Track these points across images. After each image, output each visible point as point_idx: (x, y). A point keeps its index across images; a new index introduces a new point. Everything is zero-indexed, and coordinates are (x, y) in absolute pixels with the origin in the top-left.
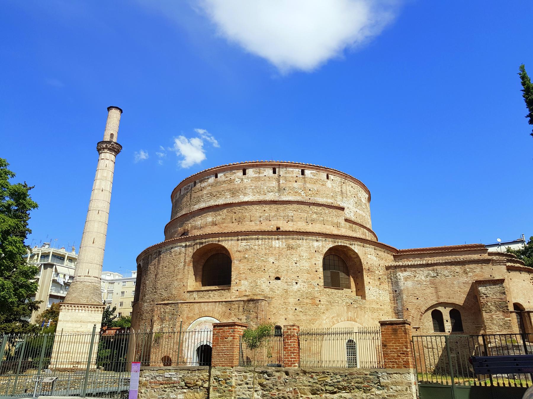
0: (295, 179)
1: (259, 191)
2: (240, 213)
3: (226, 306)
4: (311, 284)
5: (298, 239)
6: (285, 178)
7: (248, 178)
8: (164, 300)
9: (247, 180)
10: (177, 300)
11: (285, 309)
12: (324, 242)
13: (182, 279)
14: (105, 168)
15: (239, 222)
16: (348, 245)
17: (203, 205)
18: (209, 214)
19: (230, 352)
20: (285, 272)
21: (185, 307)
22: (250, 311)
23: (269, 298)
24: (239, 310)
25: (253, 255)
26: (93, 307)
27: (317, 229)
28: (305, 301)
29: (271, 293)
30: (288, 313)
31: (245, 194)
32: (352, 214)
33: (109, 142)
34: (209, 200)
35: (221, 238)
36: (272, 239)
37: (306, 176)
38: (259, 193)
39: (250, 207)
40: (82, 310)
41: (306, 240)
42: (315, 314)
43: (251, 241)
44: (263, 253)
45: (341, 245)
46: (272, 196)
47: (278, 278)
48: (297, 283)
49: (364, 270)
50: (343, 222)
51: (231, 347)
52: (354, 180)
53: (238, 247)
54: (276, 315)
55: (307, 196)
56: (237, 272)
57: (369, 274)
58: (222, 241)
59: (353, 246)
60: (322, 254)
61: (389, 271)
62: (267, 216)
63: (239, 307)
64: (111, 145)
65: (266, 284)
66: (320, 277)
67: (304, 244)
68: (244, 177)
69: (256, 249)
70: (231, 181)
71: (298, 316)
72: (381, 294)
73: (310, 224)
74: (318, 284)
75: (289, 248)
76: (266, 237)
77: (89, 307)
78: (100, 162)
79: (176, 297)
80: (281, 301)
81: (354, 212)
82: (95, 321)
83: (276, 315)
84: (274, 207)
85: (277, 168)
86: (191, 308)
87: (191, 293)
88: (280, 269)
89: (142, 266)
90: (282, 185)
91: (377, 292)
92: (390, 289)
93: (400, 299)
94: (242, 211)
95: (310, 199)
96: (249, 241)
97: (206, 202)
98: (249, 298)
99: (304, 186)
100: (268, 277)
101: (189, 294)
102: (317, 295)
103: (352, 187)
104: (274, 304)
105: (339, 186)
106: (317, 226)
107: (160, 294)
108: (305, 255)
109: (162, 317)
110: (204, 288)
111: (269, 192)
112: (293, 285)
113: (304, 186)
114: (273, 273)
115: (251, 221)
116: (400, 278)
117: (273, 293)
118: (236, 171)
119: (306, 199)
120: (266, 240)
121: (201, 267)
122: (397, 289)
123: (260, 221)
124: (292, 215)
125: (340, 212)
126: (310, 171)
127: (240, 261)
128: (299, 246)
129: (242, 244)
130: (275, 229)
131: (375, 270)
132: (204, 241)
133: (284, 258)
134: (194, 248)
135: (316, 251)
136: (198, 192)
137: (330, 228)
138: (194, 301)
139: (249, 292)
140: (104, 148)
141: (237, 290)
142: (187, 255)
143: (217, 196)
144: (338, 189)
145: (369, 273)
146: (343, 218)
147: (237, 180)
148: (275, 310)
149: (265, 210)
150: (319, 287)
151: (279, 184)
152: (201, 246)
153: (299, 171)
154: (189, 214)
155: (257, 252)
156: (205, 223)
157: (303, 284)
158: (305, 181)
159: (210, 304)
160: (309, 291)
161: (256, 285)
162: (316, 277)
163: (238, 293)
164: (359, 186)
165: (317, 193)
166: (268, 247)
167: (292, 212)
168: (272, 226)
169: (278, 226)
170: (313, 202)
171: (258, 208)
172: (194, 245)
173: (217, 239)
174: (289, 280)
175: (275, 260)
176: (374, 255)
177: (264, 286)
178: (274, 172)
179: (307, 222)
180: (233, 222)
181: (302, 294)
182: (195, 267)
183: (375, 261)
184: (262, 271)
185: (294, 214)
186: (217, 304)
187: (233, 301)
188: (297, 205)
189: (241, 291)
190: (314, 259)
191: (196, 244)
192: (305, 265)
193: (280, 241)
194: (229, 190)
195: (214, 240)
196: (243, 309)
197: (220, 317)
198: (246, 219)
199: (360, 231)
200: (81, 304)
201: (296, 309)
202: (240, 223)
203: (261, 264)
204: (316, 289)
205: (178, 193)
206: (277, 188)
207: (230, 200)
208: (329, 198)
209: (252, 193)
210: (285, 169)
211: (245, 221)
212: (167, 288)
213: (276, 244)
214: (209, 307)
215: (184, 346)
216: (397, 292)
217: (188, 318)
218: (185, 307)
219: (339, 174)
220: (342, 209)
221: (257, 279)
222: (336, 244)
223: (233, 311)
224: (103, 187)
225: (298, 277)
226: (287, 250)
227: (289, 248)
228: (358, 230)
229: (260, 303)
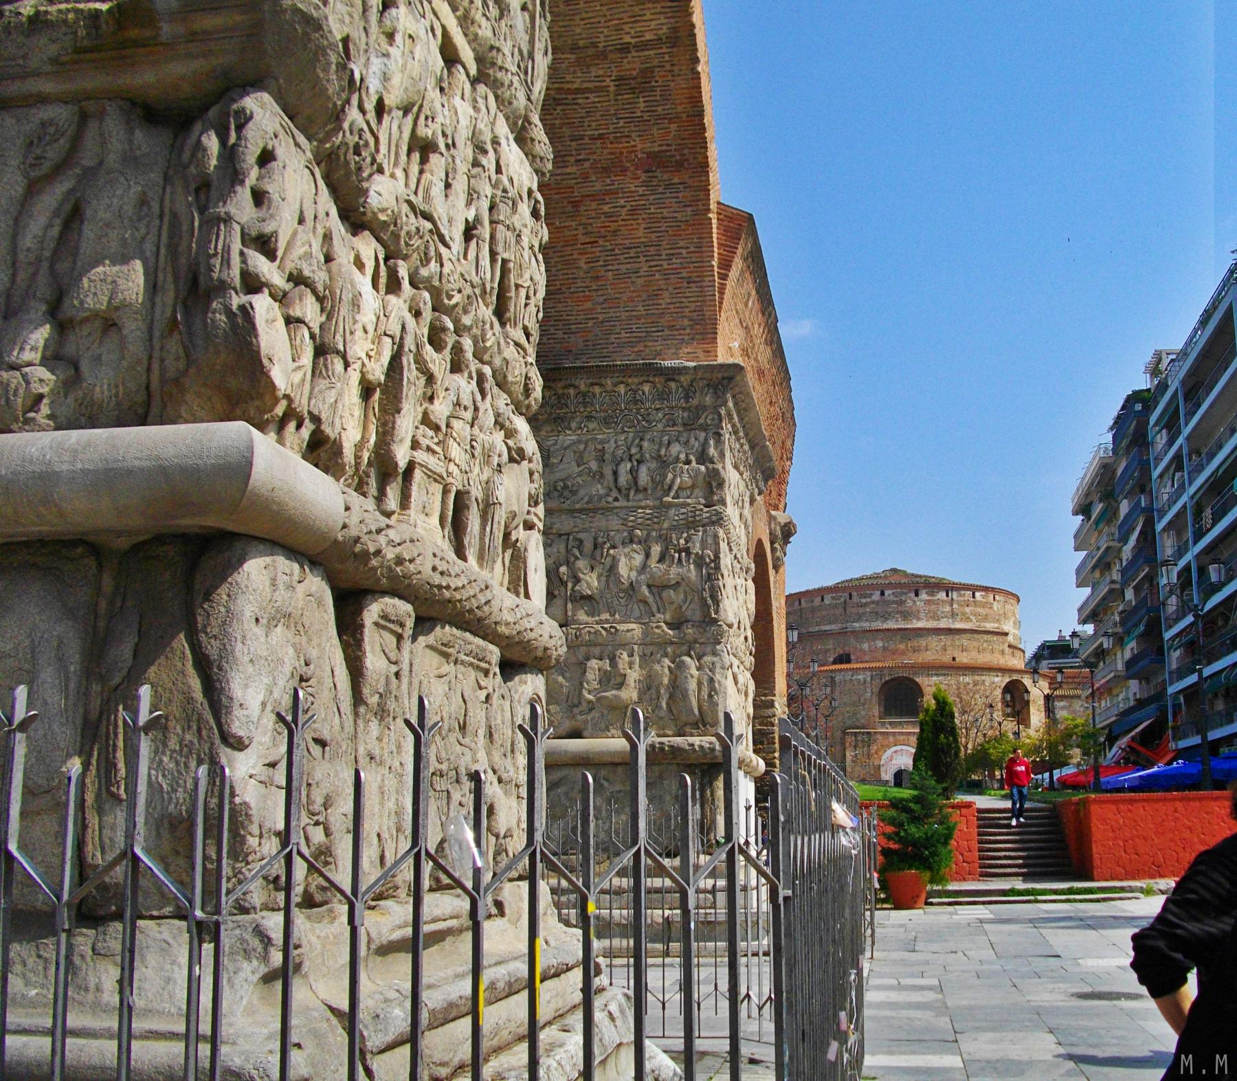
7: (921, 601)
17: (866, 625)
31: (919, 619)
38: (933, 618)
50: (1007, 650)
68: (916, 599)
178: (947, 595)
205: (819, 599)
220: (1006, 634)
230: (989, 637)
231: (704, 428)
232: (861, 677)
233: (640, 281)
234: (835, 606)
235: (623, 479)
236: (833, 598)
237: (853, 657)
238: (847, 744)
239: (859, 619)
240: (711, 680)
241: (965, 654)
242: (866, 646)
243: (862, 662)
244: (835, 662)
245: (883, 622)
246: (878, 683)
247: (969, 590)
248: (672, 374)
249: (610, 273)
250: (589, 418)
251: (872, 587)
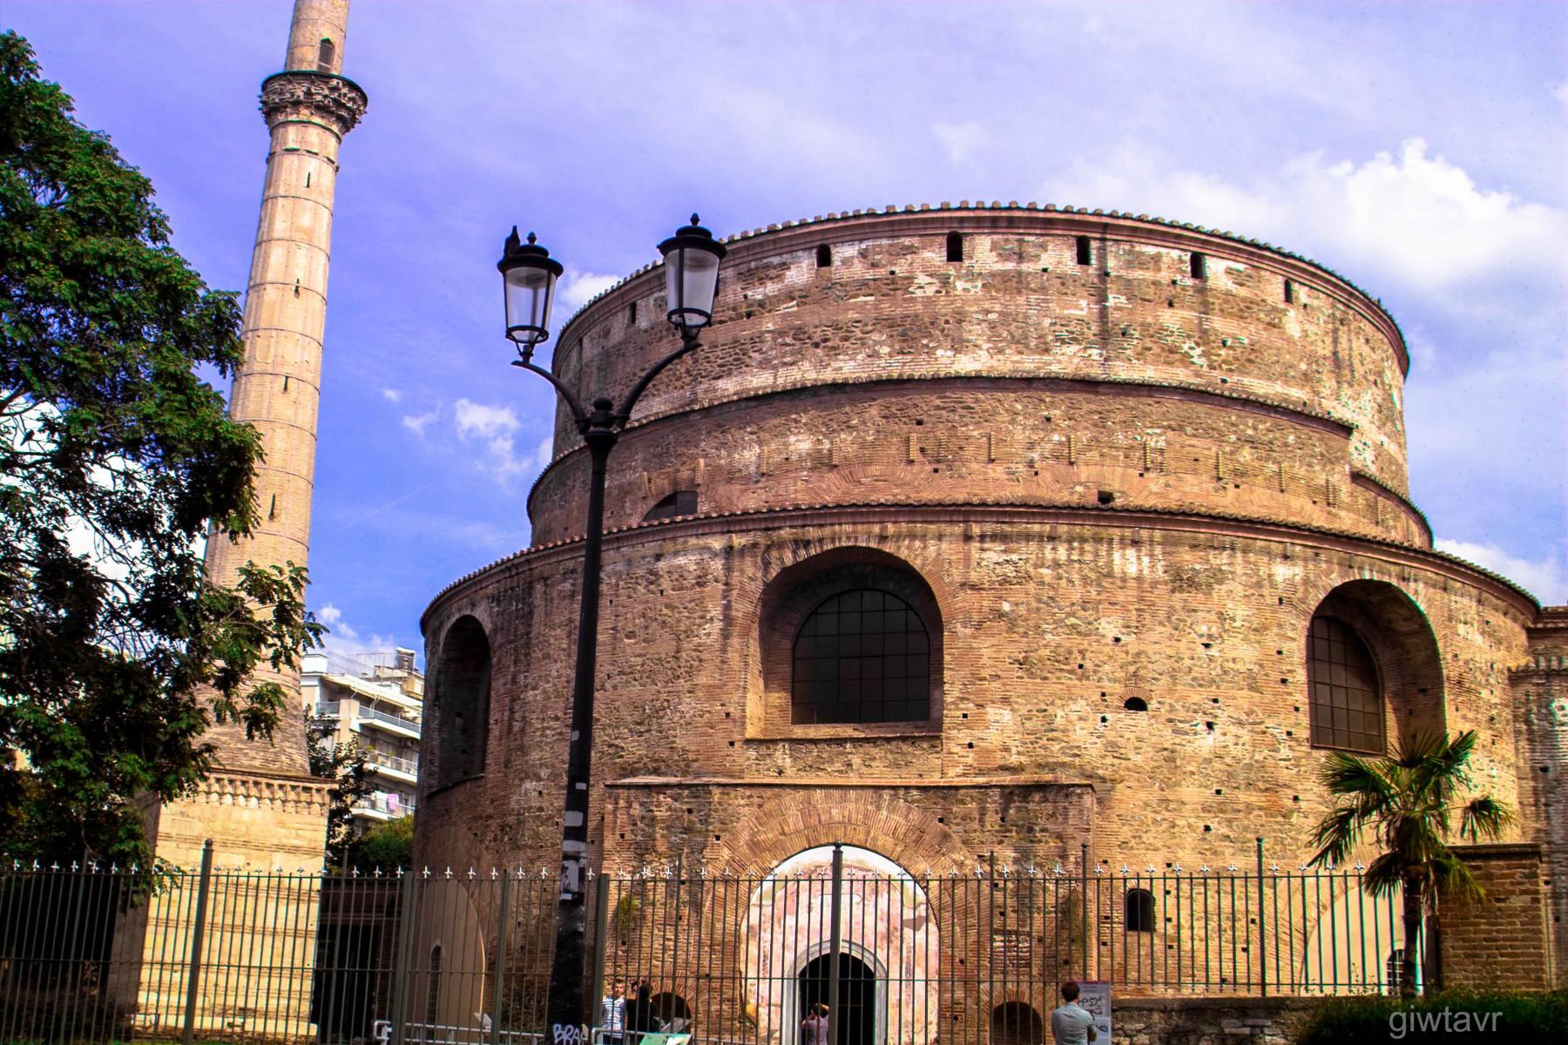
0: (1169, 292)
1: (1019, 333)
2: (941, 426)
3: (928, 804)
4: (1264, 733)
5: (1215, 548)
6: (1128, 287)
7: (971, 276)
8: (634, 773)
9: (968, 286)
10: (698, 775)
11: (1165, 825)
12: (1311, 566)
13: (720, 687)
14: (303, 192)
15: (939, 462)
16: (1394, 582)
17: (760, 380)
18: (796, 421)
19: (1527, 947)
20: (1165, 680)
21: (742, 802)
22: (1030, 830)
23: (1103, 780)
24: (981, 821)
25: (1035, 605)
26: (289, 788)
27: (1255, 508)
28: (1243, 797)
29: (1109, 760)
30: (1178, 840)
31: (959, 346)
32: (1369, 455)
33: (322, 76)
34: (787, 359)
35: (891, 528)
36: (1110, 541)
37: (1210, 284)
38: (1020, 343)
39: (986, 400)
40: (247, 797)
41: (1245, 551)
42: (1278, 848)
43: (1023, 544)
44: (1077, 595)
45: (1370, 581)
46: (1076, 361)
47: (1136, 704)
48: (1210, 726)
49: (1446, 684)
50: (1345, 488)
51: (1528, 930)
52: (1375, 312)
53: (968, 566)
54: (1132, 848)
55: (1212, 367)
56: (965, 672)
57: (1460, 699)
58: (898, 537)
59: (1412, 585)
60: (1304, 613)
61: (1520, 692)
62: (1061, 443)
63: (983, 812)
64: (327, 92)
65: (1089, 725)
66: (1298, 705)
67: (1239, 570)
69: (1047, 580)
70: (895, 285)
71: (1215, 853)
72: (1495, 780)
73: (1230, 486)
74: (1289, 733)
75: (1178, 584)
76: (1087, 531)
77: (276, 788)
78: (281, 163)
79: (696, 760)
80: (1152, 794)
81: (1375, 444)
82: (297, 843)
83: (1132, 848)
84: (1086, 407)
85: (1095, 239)
86: (767, 807)
87: (763, 750)
88: (1145, 668)
89: (488, 627)
90: (1114, 316)
91: (1485, 772)
92: (1521, 763)
93: (1558, 802)
94: (952, 416)
95: (1224, 381)
96: (1014, 546)
97: (775, 367)
98: (1023, 778)
99: (1201, 323)
100: (1097, 697)
101: (752, 753)
102: (1285, 775)
103: (1367, 341)
104: (1122, 806)
105: (1327, 333)
106: (1254, 497)
107: (610, 746)
108: (1240, 612)
109: (639, 838)
110: (799, 731)
111: (1063, 342)
112: (1196, 734)
113: (1201, 323)
114: (1115, 681)
115: (992, 461)
116: (1564, 719)
117: (1116, 762)
118: (916, 241)
119: (1211, 379)
120: (1087, 547)
121: (787, 644)
122: (1549, 763)
123: (1031, 464)
124: (1161, 444)
125: (1335, 440)
126: (1224, 264)
127: (979, 626)
128: (1219, 576)
129: (985, 555)
130: (1092, 499)
131: (1480, 684)
132: (812, 533)
133: (1161, 623)
134: (767, 565)
135: (1281, 601)
136: (731, 319)
137: (1302, 507)
138: (778, 781)
139: (1019, 753)
140: (297, 104)
141: (970, 746)
142: (735, 593)
143: (829, 344)
144: (1325, 350)
145: (1459, 694)
146: (1347, 468)
147: (922, 279)
148: (1126, 828)
149: (1048, 419)
150: (1293, 743)
151: (1103, 314)
152: (803, 554)
153: (1181, 261)
154: (692, 418)
155: (1051, 594)
156: (777, 459)
157: (1234, 729)
158: (1205, 304)
159: (852, 793)
160: (1257, 757)
161: (1047, 727)
162: (1281, 704)
163: (971, 755)
164: (1386, 340)
165: (1250, 358)
166: (1093, 576)
167: (1158, 431)
168: (1079, 489)
169: (1107, 489)
170: (1244, 396)
171: (1019, 407)
172: (768, 548)
173: (876, 529)
174: (1182, 714)
175: (1124, 630)
176: (1476, 624)
177: (1080, 735)
178: (1083, 258)
179: (1219, 479)
180: (911, 462)
181: (1230, 769)
182: (764, 640)
183: (1480, 649)
184: (1071, 672)
185: (1168, 442)
186: (886, 795)
187: (957, 788)
188: (1179, 404)
189: (988, 751)
190: (1275, 630)
191: (780, 545)
192: (1242, 653)
193: (1145, 550)
194: (890, 323)
195: (863, 535)
196: (1003, 819)
197: (899, 849)
198: (969, 452)
199: (1399, 525)
200: (243, 773)
201: (1207, 828)
202: (942, 466)
203: (1067, 644)
204: (1282, 751)
205: (621, 320)
206: (1095, 328)
207: (891, 365)
208: (1293, 382)
209: (989, 340)
210: (1127, 247)
211: (964, 462)
212: (648, 719)
213: (1128, 562)
214: (852, 806)
215: (743, 957)
216: (1551, 775)
217: (755, 846)
218: (742, 802)
219: (1328, 282)
220: (1346, 429)
221: (1052, 703)
222: (1355, 575)
223: (955, 828)
224: (299, 274)
225: (1215, 701)
226: (1173, 591)
227: (1181, 581)
228: (1391, 523)
229: (1075, 799)
230: (1264, 425)
238: (608, 844)
239: (737, 362)
241: (1154, 482)
245: (821, 365)
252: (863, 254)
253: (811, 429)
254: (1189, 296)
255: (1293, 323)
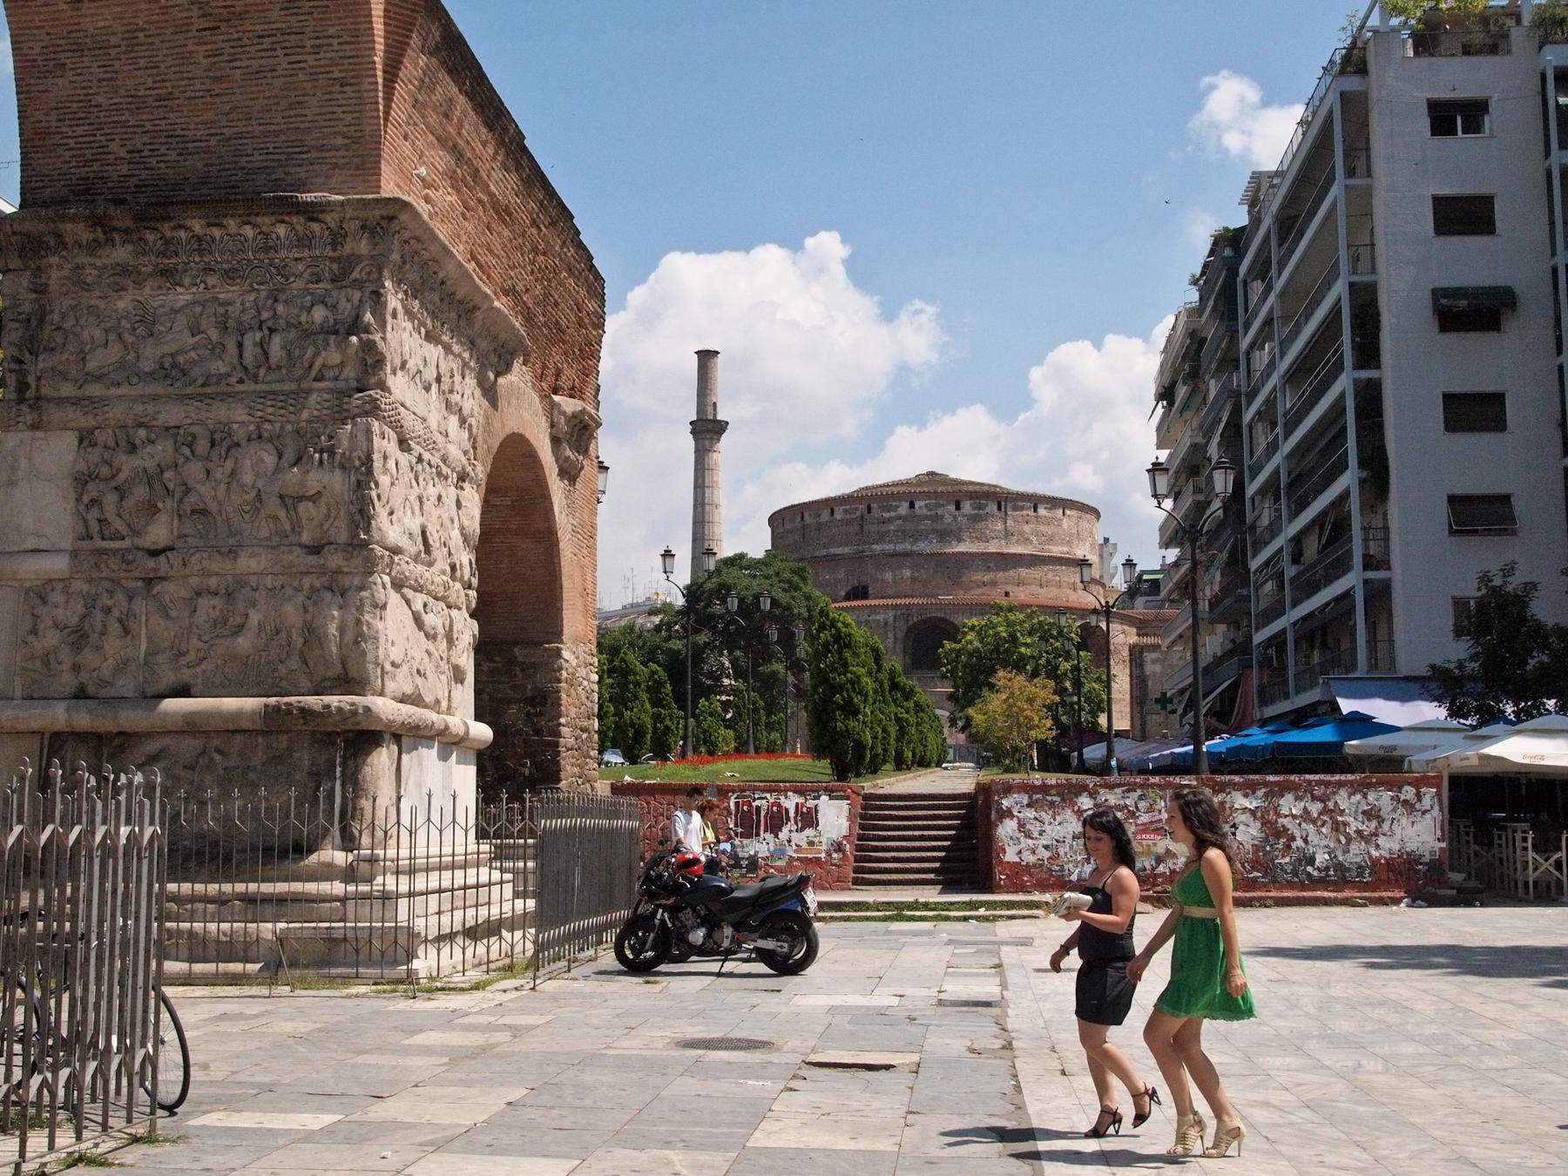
7: (964, 516)
17: (890, 547)
31: (960, 540)
68: (957, 513)
70: (937, 518)
144: (1074, 531)
178: (999, 509)
231: (359, 284)
232: (880, 617)
233: (278, 83)
234: (849, 523)
235: (250, 353)
236: (846, 511)
237: (871, 591)
239: (880, 540)
240: (359, 622)
242: (889, 576)
243: (883, 598)
244: (847, 598)
245: (912, 544)
246: (902, 625)
247: (1029, 501)
248: (313, 212)
249: (238, 71)
250: (207, 270)
251: (898, 497)
252: (926, 505)
253: (910, 568)
254: (1034, 520)
255: (1065, 523)
